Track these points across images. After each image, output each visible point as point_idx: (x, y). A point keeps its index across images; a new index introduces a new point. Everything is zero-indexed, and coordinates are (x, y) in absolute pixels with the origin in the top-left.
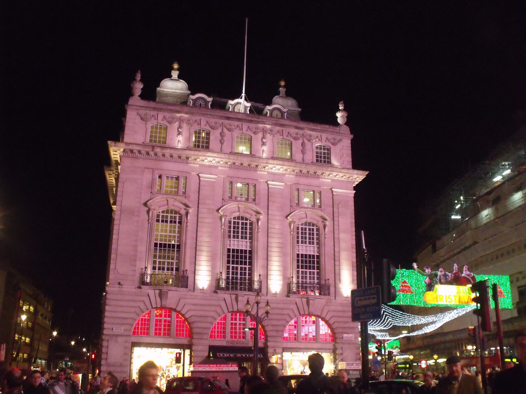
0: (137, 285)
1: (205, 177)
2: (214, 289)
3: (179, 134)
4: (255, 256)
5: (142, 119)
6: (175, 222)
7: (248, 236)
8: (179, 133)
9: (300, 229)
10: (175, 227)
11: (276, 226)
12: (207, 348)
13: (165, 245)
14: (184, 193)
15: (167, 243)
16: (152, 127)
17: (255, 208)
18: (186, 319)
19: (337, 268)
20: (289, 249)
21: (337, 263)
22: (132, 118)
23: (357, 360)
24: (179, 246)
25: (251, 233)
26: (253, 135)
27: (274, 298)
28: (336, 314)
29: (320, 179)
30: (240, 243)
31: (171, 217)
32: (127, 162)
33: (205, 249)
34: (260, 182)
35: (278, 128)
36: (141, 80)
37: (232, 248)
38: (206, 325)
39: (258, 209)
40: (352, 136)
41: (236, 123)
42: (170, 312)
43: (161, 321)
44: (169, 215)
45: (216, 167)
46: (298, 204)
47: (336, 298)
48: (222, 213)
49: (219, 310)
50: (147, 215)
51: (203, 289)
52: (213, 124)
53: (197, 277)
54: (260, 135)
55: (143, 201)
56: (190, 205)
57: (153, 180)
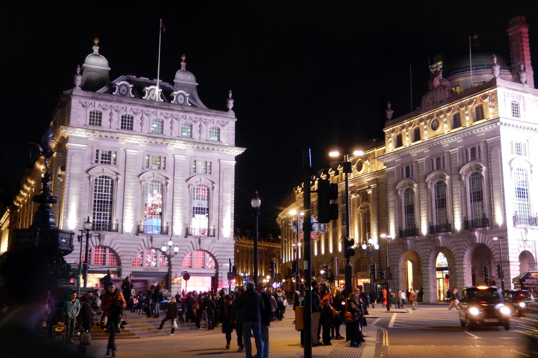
1: (130, 152)
5: (83, 106)
13: (101, 201)
15: (103, 200)
16: (91, 113)
17: (165, 175)
19: (220, 217)
21: (220, 214)
24: (111, 202)
26: (165, 120)
27: (177, 239)
33: (129, 204)
40: (236, 120)
41: (152, 110)
42: (105, 248)
45: (138, 144)
49: (139, 247)
52: (135, 111)
53: (124, 224)
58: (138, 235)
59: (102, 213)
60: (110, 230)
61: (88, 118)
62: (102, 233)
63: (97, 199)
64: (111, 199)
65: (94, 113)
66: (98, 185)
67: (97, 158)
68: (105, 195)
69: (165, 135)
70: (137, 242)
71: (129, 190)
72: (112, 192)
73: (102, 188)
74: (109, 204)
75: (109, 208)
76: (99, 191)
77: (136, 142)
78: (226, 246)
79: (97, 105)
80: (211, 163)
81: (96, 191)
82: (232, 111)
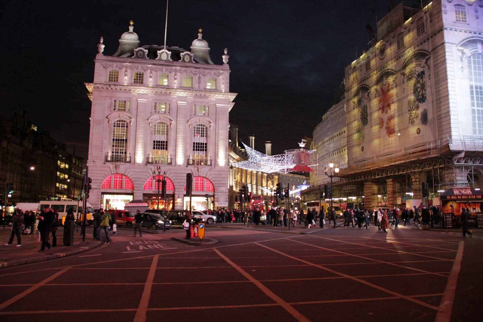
0: (103, 162)
2: (145, 163)
3: (125, 76)
4: (169, 144)
5: (104, 67)
6: (124, 127)
7: (166, 133)
8: (126, 75)
9: (196, 128)
10: (124, 129)
11: (181, 127)
12: (142, 195)
13: (119, 139)
14: (129, 110)
15: (120, 138)
16: (110, 72)
17: (169, 117)
18: (130, 180)
19: (217, 150)
20: (189, 139)
22: (98, 66)
23: (226, 201)
24: (126, 140)
25: (167, 132)
26: (169, 74)
28: (214, 176)
29: (209, 99)
31: (122, 124)
32: (96, 94)
35: (184, 69)
38: (140, 183)
41: (160, 67)
42: (122, 176)
43: (117, 181)
44: (121, 123)
46: (195, 114)
47: (216, 167)
48: (150, 121)
49: (148, 174)
50: (108, 123)
51: (139, 163)
52: (145, 68)
53: (136, 157)
54: (173, 73)
55: (106, 116)
56: (132, 117)
57: (111, 103)
58: (147, 165)
59: (120, 148)
60: (126, 162)
61: (108, 76)
62: (118, 163)
63: (115, 138)
65: (113, 72)
67: (115, 106)
68: (121, 135)
71: (140, 131)
74: (125, 142)
75: (124, 145)
76: (117, 132)
77: (145, 92)
79: (114, 66)
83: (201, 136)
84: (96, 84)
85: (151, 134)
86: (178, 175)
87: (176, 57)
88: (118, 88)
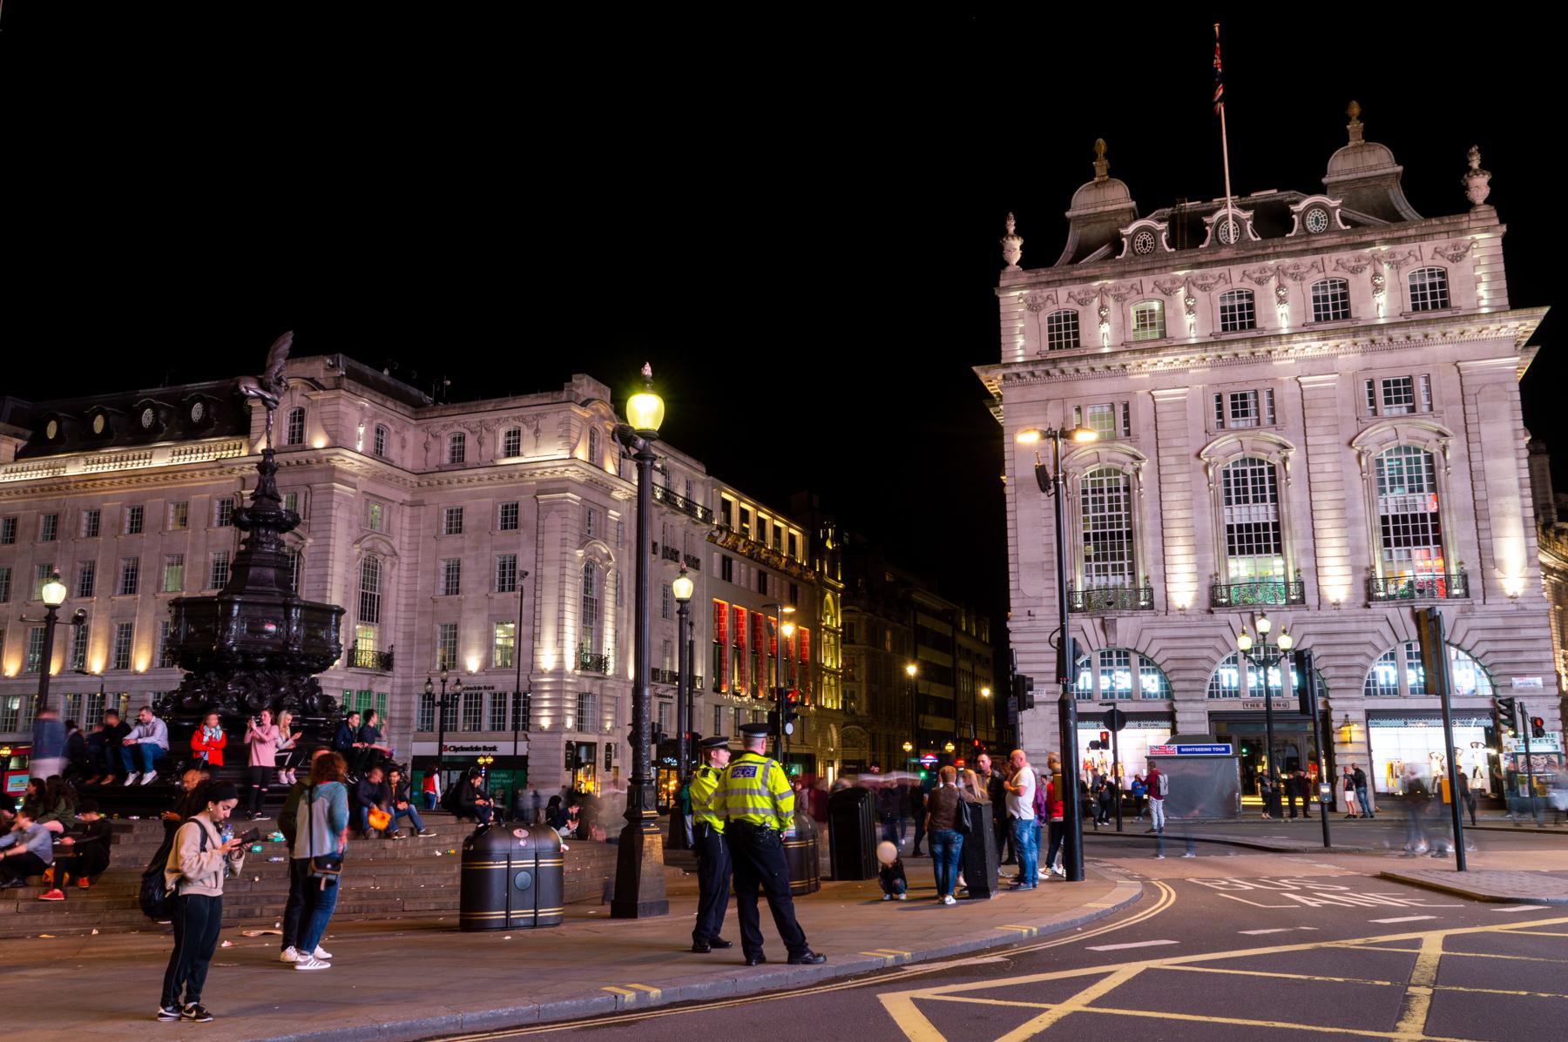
2: (1206, 606)
4: (1286, 534)
7: (1268, 494)
8: (1103, 320)
11: (1325, 466)
13: (1104, 534)
16: (1050, 320)
24: (1130, 534)
30: (1254, 510)
32: (1011, 395)
34: (1282, 383)
36: (1018, 233)
37: (1236, 522)
39: (1282, 439)
40: (1504, 228)
41: (1216, 271)
42: (1126, 655)
52: (1168, 285)
56: (1141, 454)
64: (1129, 524)
65: (1059, 319)
66: (1090, 496)
68: (1111, 518)
69: (1263, 329)
70: (1212, 632)
72: (1128, 508)
73: (1102, 500)
76: (1095, 510)
78: (1516, 622)
79: (1063, 298)
80: (1428, 379)
81: (1085, 511)
82: (1486, 207)
83: (1412, 490)
84: (1008, 365)
85: (1216, 504)
86: (1336, 639)
87: (1274, 223)
88: (1083, 366)
